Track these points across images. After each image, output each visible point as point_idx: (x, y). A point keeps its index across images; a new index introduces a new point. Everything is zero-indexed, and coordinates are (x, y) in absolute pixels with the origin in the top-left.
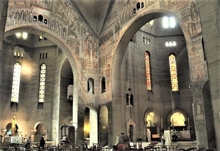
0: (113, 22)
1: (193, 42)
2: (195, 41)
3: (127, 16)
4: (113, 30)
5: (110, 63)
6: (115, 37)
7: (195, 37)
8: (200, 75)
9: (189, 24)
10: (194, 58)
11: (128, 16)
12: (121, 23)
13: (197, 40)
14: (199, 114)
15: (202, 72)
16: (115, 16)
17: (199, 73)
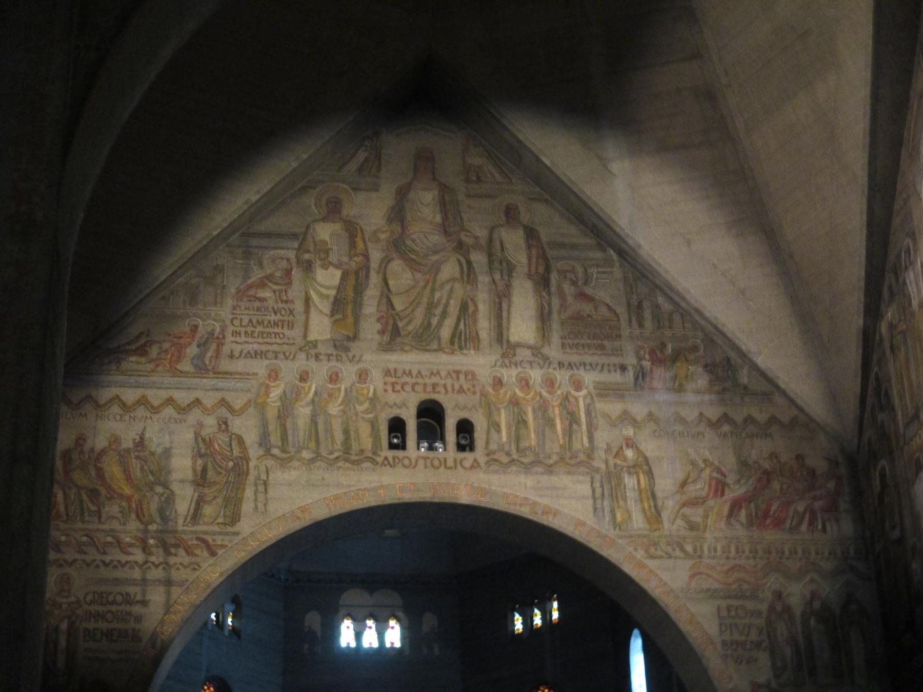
0: (182, 397)
3: (329, 430)
4: (167, 453)
6: (196, 516)
11: (339, 437)
12: (264, 441)
16: (201, 370)
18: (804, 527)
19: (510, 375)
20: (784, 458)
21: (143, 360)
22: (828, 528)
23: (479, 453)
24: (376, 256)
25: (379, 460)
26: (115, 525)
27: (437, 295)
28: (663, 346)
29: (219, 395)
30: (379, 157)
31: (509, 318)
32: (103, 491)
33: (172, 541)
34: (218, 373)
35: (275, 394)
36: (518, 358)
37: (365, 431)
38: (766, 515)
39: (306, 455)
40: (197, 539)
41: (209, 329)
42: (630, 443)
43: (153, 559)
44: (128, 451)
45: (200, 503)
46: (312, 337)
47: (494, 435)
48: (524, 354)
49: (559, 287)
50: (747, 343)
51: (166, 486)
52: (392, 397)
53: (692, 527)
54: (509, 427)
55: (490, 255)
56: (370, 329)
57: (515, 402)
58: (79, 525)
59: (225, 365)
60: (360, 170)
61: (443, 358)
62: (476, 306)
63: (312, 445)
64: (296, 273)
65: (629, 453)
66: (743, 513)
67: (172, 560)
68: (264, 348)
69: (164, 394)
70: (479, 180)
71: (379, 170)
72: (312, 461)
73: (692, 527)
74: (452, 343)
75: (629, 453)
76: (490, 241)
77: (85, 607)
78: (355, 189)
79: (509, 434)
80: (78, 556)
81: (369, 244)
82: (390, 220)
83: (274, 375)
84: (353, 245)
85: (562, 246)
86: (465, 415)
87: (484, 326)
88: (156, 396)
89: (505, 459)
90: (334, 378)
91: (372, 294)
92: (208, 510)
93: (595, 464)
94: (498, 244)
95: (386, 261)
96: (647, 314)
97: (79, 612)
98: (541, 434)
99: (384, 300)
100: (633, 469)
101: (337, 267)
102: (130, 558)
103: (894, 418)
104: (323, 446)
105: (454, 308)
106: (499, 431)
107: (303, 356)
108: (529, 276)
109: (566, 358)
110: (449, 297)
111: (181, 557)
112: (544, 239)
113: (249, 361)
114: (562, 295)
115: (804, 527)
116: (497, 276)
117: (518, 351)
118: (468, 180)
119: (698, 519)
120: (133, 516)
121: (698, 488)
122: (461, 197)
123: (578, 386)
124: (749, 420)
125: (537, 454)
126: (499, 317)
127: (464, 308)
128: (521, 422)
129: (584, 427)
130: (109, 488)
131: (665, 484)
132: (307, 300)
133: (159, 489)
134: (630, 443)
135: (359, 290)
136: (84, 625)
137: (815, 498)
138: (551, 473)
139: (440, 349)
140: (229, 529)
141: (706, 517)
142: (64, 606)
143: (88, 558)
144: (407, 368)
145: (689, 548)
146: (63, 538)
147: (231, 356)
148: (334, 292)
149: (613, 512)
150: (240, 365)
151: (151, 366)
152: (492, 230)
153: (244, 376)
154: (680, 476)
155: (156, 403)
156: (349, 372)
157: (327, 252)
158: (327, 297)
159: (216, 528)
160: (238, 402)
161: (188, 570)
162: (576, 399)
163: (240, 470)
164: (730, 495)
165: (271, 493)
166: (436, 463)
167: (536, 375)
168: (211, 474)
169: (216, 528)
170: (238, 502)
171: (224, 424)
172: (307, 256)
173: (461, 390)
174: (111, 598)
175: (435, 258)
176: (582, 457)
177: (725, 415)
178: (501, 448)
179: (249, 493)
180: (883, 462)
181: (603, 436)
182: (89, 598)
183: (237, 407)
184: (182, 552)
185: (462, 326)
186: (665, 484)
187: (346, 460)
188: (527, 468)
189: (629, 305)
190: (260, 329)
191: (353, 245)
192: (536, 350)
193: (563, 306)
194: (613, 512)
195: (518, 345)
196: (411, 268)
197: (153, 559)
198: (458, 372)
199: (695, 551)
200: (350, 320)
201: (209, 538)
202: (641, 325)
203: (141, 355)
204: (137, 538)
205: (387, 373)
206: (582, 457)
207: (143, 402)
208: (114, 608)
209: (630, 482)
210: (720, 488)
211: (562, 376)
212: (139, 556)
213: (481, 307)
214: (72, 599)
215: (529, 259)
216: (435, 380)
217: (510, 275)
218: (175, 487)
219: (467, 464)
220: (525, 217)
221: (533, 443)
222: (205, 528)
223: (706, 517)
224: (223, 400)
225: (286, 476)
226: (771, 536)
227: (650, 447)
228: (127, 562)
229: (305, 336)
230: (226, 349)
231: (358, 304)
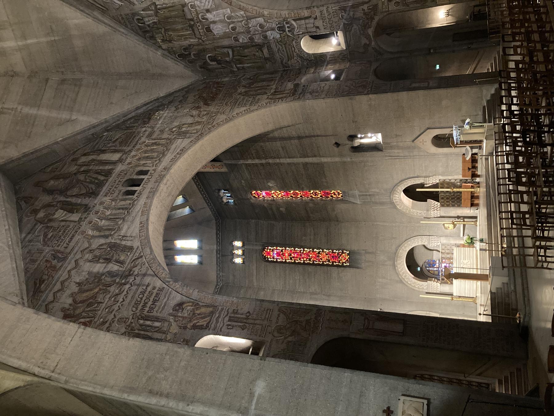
3: (115, 215)
6: (122, 263)
40: (132, 263)
45: (118, 261)
50: (154, 96)
58: (100, 312)
67: (136, 273)
77: (138, 311)
99: (79, 196)
102: (126, 291)
105: (95, 176)
120: (108, 288)
132: (62, 221)
142: (132, 321)
144: (108, 189)
146: (102, 320)
159: (131, 255)
160: (86, 245)
161: (143, 266)
165: (129, 235)
170: (125, 246)
171: (91, 251)
174: (139, 299)
182: (134, 309)
183: (88, 246)
184: (134, 269)
185: (103, 174)
186: (190, 120)
191: (53, 206)
197: (131, 280)
207: (62, 283)
208: (144, 298)
224: (81, 251)
228: (127, 292)
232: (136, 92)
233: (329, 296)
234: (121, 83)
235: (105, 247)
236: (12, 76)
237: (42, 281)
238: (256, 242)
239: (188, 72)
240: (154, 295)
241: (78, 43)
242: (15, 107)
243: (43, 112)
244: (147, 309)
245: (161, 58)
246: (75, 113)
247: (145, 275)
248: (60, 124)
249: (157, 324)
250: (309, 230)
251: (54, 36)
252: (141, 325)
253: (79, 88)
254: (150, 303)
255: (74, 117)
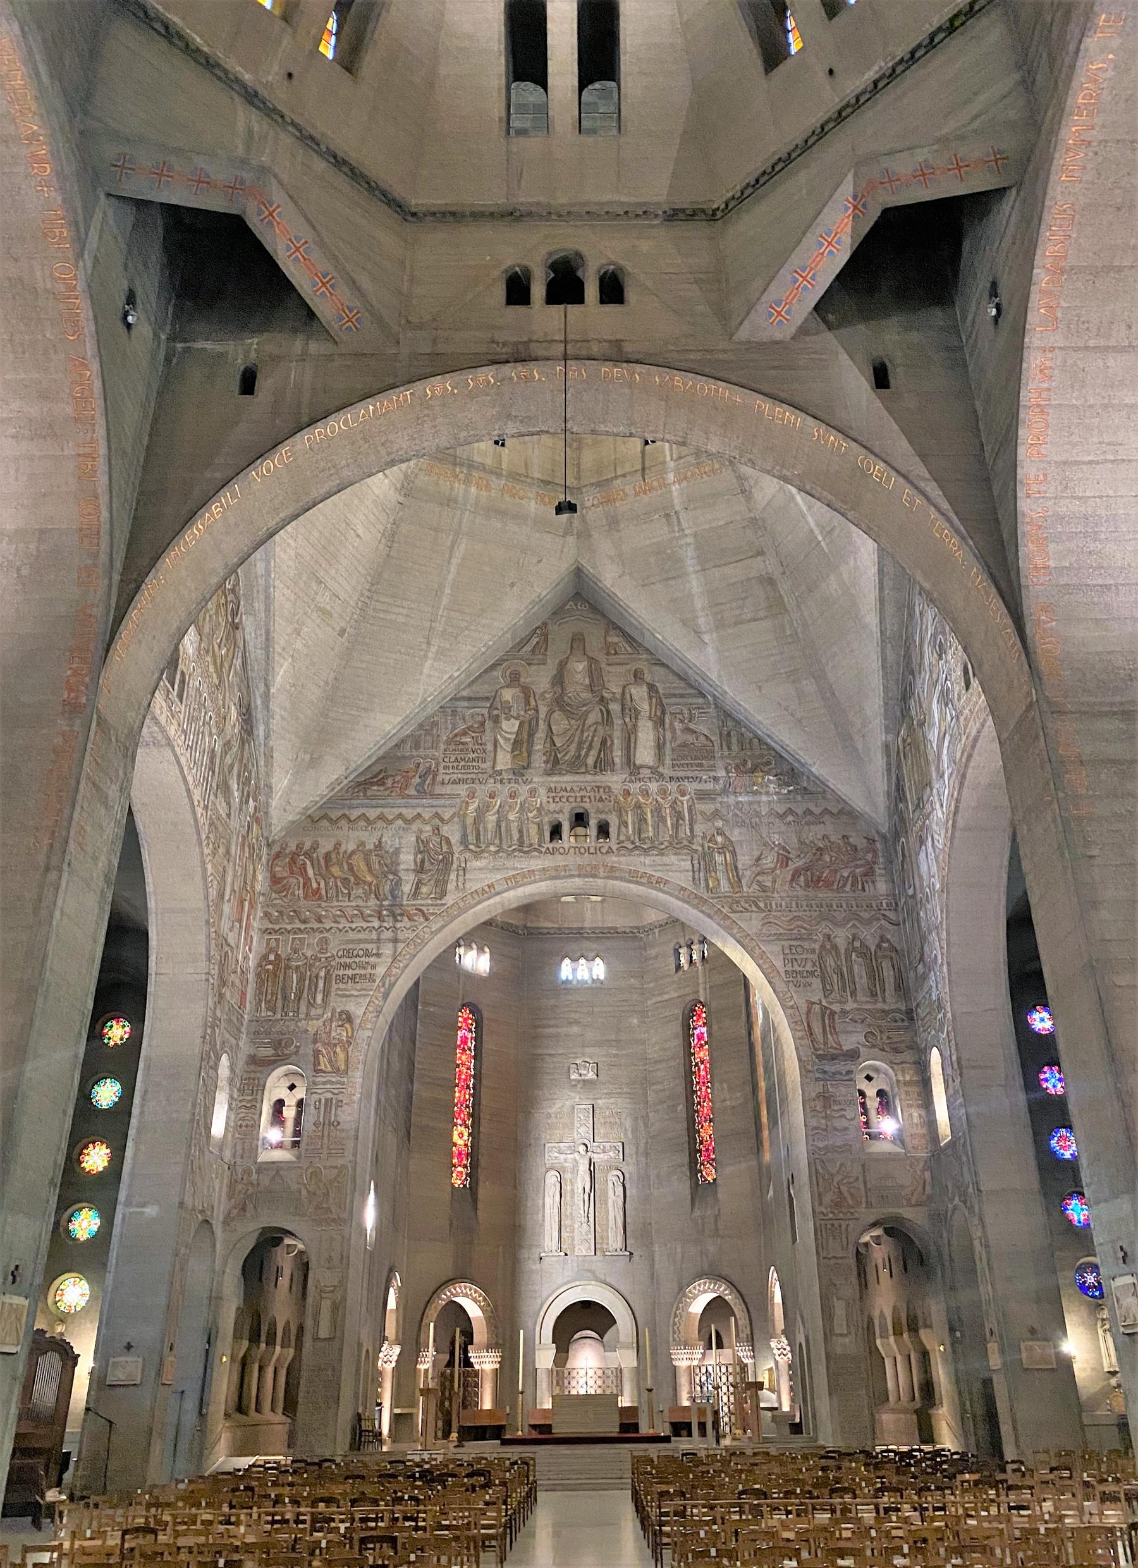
0: (409, 813)
1: (825, 1072)
2: (834, 1074)
3: (508, 830)
4: (397, 851)
5: (357, 1009)
6: (416, 893)
7: (834, 1058)
8: (846, 1194)
9: (814, 1003)
10: (825, 1130)
11: (516, 836)
12: (464, 841)
13: (841, 1073)
14: (841, 1335)
15: (855, 1184)
16: (421, 793)
17: (844, 1189)
18: (848, 888)
19: (634, 787)
20: (833, 838)
21: (382, 788)
22: (867, 888)
23: (613, 842)
24: (543, 711)
25: (543, 850)
26: (361, 903)
27: (586, 735)
28: (745, 761)
29: (434, 810)
30: (546, 641)
31: (635, 748)
32: (352, 879)
33: (399, 911)
34: (433, 795)
35: (472, 808)
36: (641, 776)
37: (533, 830)
38: (819, 880)
39: (493, 848)
41: (427, 765)
42: (720, 832)
43: (385, 924)
44: (370, 851)
46: (498, 768)
47: (623, 829)
48: (645, 772)
49: (671, 724)
50: (804, 757)
51: (395, 873)
52: (552, 807)
53: (764, 889)
54: (634, 823)
55: (623, 706)
56: (539, 761)
57: (638, 806)
59: (438, 790)
60: (533, 651)
61: (589, 778)
62: (612, 741)
63: (497, 841)
64: (488, 724)
65: (719, 839)
66: (802, 878)
67: (399, 925)
68: (465, 777)
69: (396, 811)
70: (616, 653)
71: (546, 650)
72: (497, 852)
73: (764, 889)
74: (595, 767)
75: (719, 839)
76: (623, 694)
77: (337, 959)
78: (529, 664)
79: (634, 828)
80: (334, 925)
81: (539, 702)
82: (553, 685)
83: (472, 795)
84: (528, 703)
85: (675, 695)
86: (603, 816)
87: (618, 755)
88: (390, 813)
89: (631, 846)
90: (513, 795)
91: (541, 735)
92: (424, 889)
93: (694, 847)
94: (628, 696)
95: (550, 713)
96: (734, 740)
97: (333, 963)
98: (656, 828)
100: (722, 850)
101: (516, 719)
103: (907, 807)
104: (504, 842)
106: (627, 827)
107: (492, 781)
108: (650, 718)
109: (672, 774)
110: (593, 736)
111: (406, 922)
112: (661, 691)
113: (455, 786)
114: (673, 730)
115: (848, 888)
116: (627, 720)
117: (641, 771)
118: (608, 654)
119: (769, 884)
120: (373, 896)
121: (769, 860)
122: (603, 665)
123: (683, 795)
124: (808, 812)
125: (652, 842)
126: (629, 747)
127: (604, 742)
128: (642, 820)
129: (687, 822)
130: (356, 877)
131: (744, 860)
132: (496, 742)
133: (391, 877)
134: (720, 832)
135: (531, 735)
136: (336, 972)
137: (857, 866)
138: (663, 854)
139: (587, 772)
140: (439, 902)
141: (774, 882)
143: (341, 926)
145: (762, 905)
147: (443, 783)
148: (514, 736)
149: (706, 880)
150: (448, 789)
151: (387, 792)
152: (624, 687)
153: (452, 796)
154: (756, 853)
155: (391, 817)
156: (524, 790)
157: (510, 708)
158: (509, 739)
162: (682, 802)
163: (447, 862)
164: (792, 866)
165: (467, 876)
166: (582, 850)
167: (653, 787)
168: (427, 864)
169: (430, 902)
172: (495, 712)
173: (601, 800)
174: (355, 953)
175: (585, 709)
176: (685, 843)
177: (790, 811)
178: (628, 839)
179: (453, 876)
180: (903, 839)
181: (699, 829)
182: (340, 953)
184: (406, 919)
187: (520, 851)
188: (646, 852)
189: (721, 734)
190: (462, 763)
191: (528, 703)
192: (654, 770)
193: (674, 738)
194: (706, 880)
195: (642, 767)
196: (568, 717)
197: (385, 924)
198: (599, 787)
199: (766, 906)
200: (525, 754)
201: (424, 908)
202: (729, 748)
203: (379, 785)
204: (373, 910)
205: (550, 790)
206: (685, 843)
207: (381, 817)
208: (357, 960)
209: (719, 859)
210: (784, 860)
211: (672, 787)
212: (376, 923)
213: (615, 741)
214: (329, 954)
215: (650, 706)
216: (583, 793)
217: (636, 718)
218: (402, 874)
219: (604, 851)
220: (648, 677)
221: (651, 834)
222: (422, 902)
223: (774, 882)
225: (478, 863)
226: (824, 895)
227: (736, 835)
229: (493, 767)
230: (439, 779)
231: (531, 742)
232: (800, 721)
233: (647, 1155)
234: (809, 686)
235: (445, 849)
236: (743, 492)
237: (381, 783)
238: (711, 987)
239: (881, 801)
240: (362, 972)
241: (832, 585)
242: (687, 532)
243: (695, 584)
244: (341, 973)
245: (879, 744)
246: (715, 635)
247: (395, 941)
248: (684, 623)
249: (319, 998)
250: (739, 1095)
251: (824, 539)
252: (317, 976)
253: (766, 617)
254: (350, 972)
255: (706, 638)
